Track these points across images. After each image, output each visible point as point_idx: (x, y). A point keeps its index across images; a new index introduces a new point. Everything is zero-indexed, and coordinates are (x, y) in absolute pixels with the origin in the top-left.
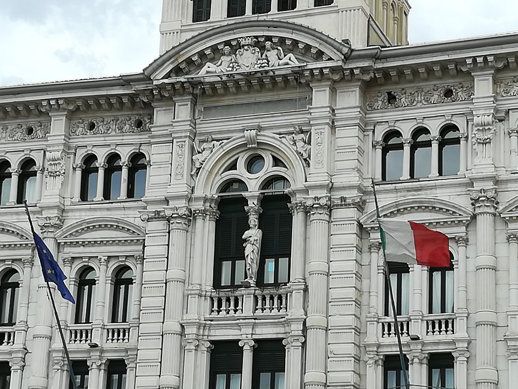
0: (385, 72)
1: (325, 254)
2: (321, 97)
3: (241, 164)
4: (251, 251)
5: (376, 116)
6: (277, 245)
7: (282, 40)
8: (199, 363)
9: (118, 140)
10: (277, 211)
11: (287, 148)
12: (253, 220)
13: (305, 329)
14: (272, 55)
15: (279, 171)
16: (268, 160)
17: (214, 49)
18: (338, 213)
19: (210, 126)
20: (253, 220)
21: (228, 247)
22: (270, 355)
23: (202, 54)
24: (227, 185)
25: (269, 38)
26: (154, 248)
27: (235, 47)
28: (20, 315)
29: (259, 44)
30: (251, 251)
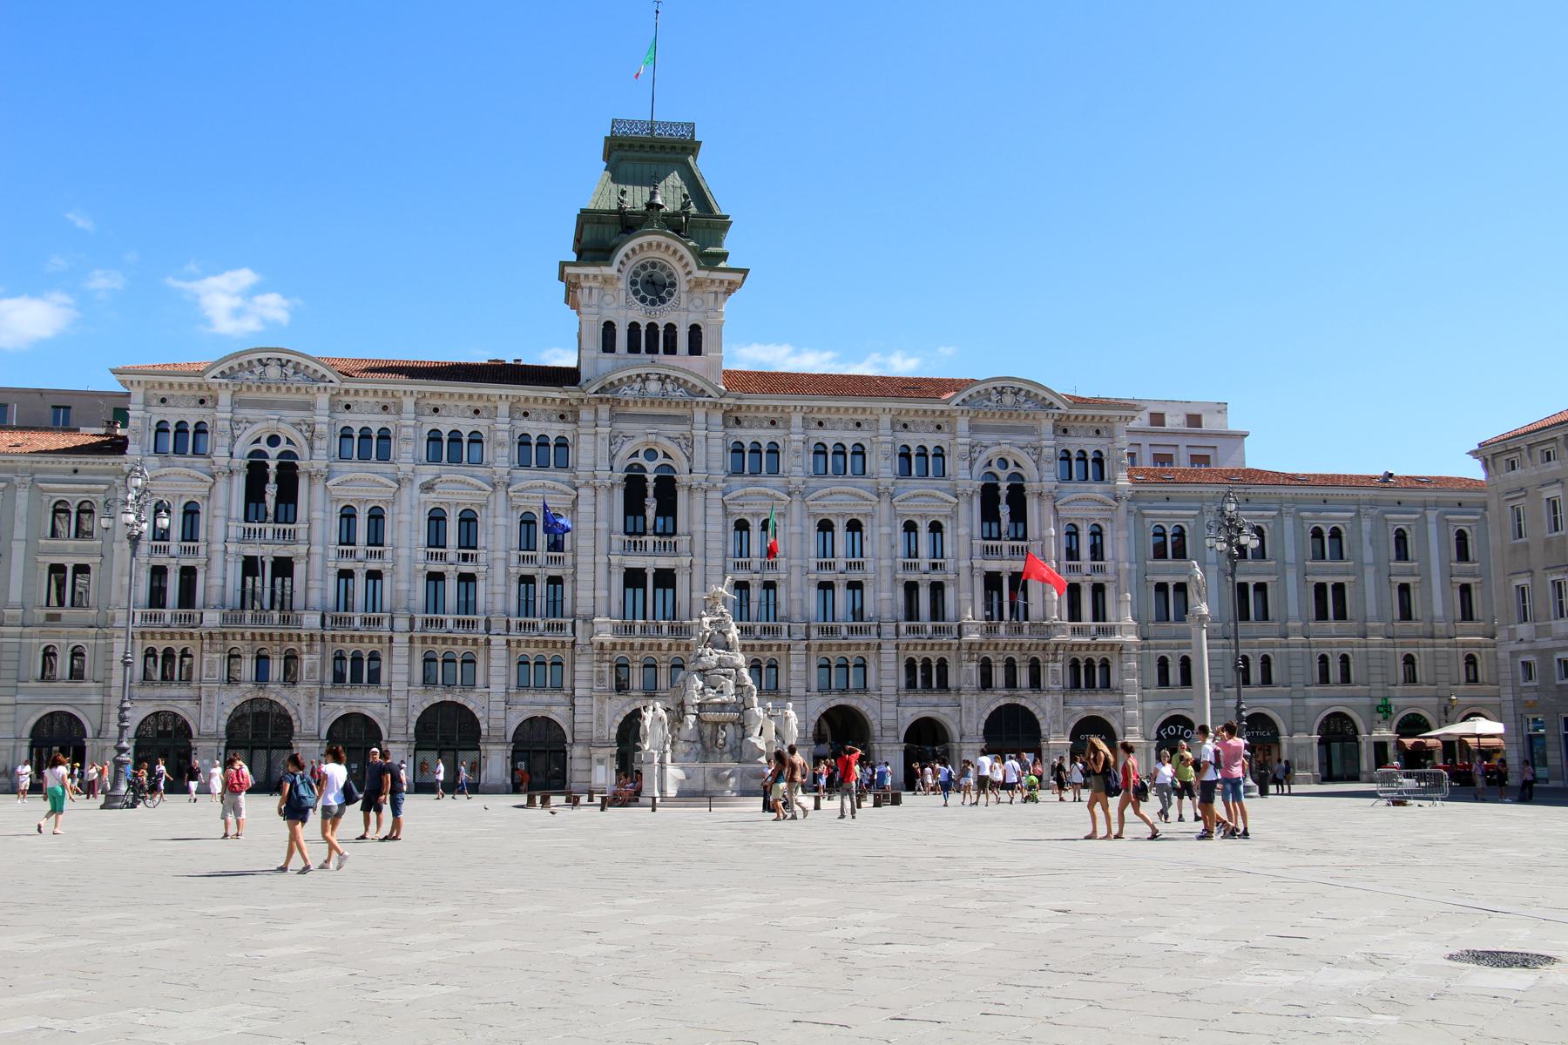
0: (740, 407)
1: (702, 518)
2: (699, 415)
3: (641, 454)
4: (650, 512)
5: (729, 431)
6: (668, 507)
7: (677, 379)
8: (618, 580)
9: (547, 425)
10: (667, 488)
11: (673, 449)
12: (651, 492)
14: (669, 387)
15: (667, 461)
16: (660, 455)
17: (629, 377)
18: (710, 495)
19: (625, 427)
20: (651, 492)
21: (633, 505)
22: (666, 579)
23: (620, 380)
24: (630, 468)
25: (668, 376)
26: (584, 508)
27: (646, 379)
28: (481, 542)
29: (662, 379)
30: (650, 512)
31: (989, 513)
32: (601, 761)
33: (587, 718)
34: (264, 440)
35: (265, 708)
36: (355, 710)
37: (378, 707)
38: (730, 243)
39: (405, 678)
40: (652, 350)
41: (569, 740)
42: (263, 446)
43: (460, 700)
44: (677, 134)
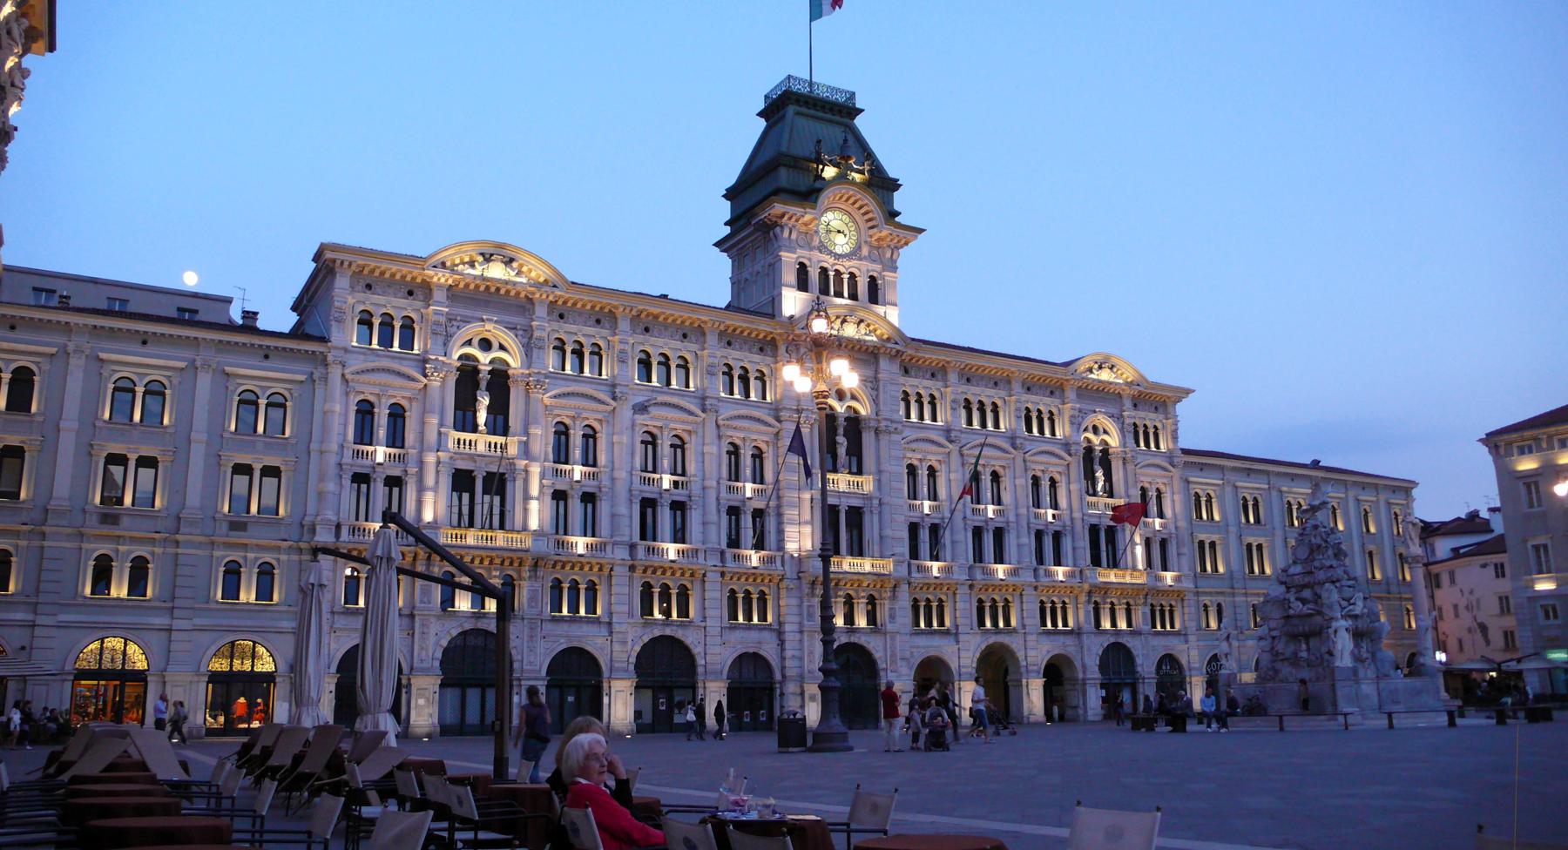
12: (841, 431)
13: (880, 504)
20: (841, 431)
31: (1090, 476)
32: (813, 698)
33: (797, 653)
34: (475, 341)
35: (480, 641)
36: (575, 644)
37: (600, 641)
38: (899, 200)
39: (626, 608)
40: (839, 294)
41: (778, 677)
42: (474, 351)
43: (678, 634)
44: (841, 99)
